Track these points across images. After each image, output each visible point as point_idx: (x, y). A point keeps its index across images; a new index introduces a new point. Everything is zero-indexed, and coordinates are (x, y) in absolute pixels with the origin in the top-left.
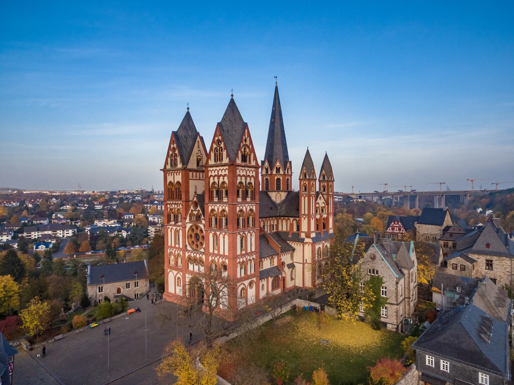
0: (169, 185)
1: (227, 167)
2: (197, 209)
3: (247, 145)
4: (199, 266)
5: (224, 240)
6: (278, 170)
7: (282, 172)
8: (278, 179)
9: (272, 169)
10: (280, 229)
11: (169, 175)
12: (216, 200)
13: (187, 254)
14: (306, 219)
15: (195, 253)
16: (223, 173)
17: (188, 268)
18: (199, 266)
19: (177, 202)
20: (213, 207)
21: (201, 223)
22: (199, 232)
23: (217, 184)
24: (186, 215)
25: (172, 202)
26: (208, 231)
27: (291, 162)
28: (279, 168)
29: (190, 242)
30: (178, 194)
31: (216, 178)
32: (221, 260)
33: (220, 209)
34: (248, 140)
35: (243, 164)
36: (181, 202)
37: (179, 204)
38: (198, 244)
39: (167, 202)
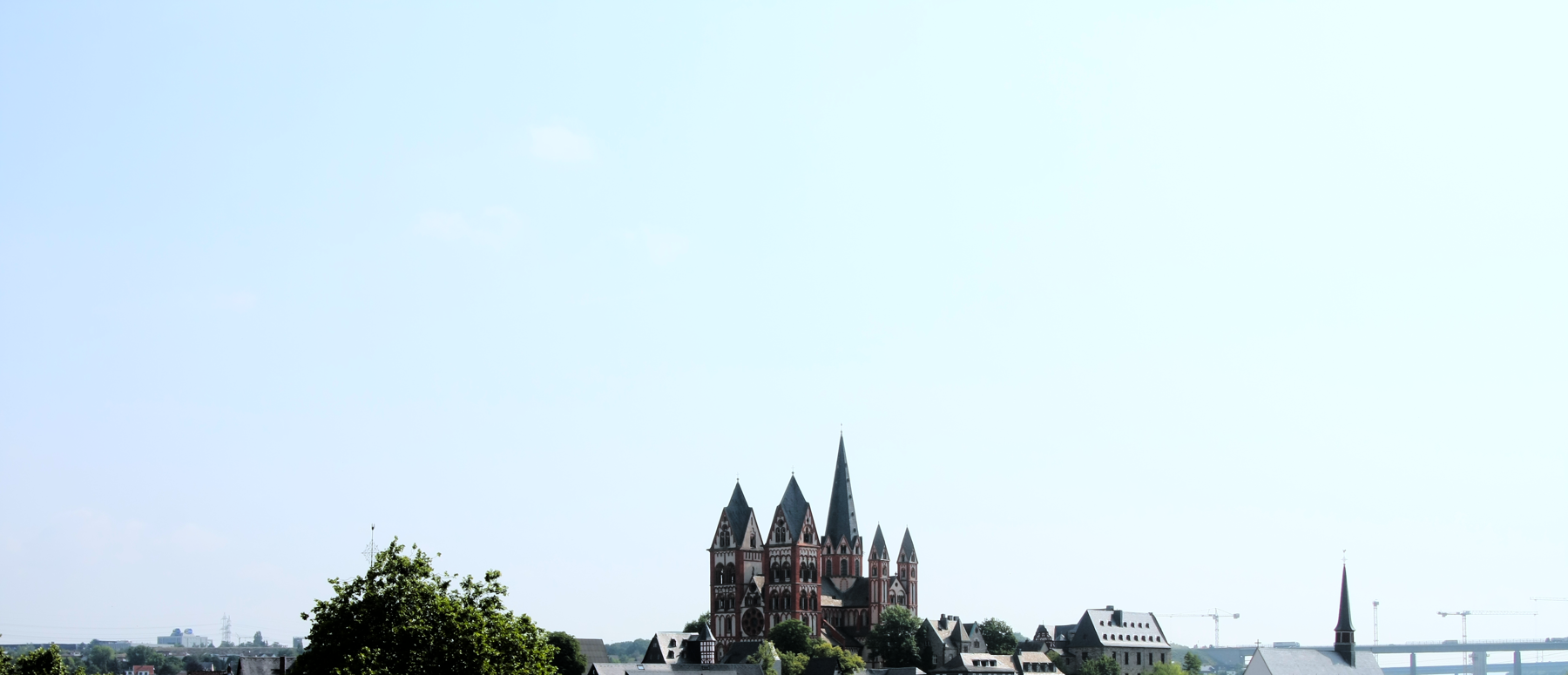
3: (808, 525)
6: (843, 549)
7: (848, 552)
8: (844, 561)
9: (835, 548)
10: (846, 624)
12: (777, 580)
14: (877, 608)
16: (786, 553)
21: (760, 606)
22: (756, 616)
24: (741, 599)
27: (861, 538)
28: (845, 547)
31: (778, 560)
33: (783, 589)
34: (810, 519)
35: (806, 545)
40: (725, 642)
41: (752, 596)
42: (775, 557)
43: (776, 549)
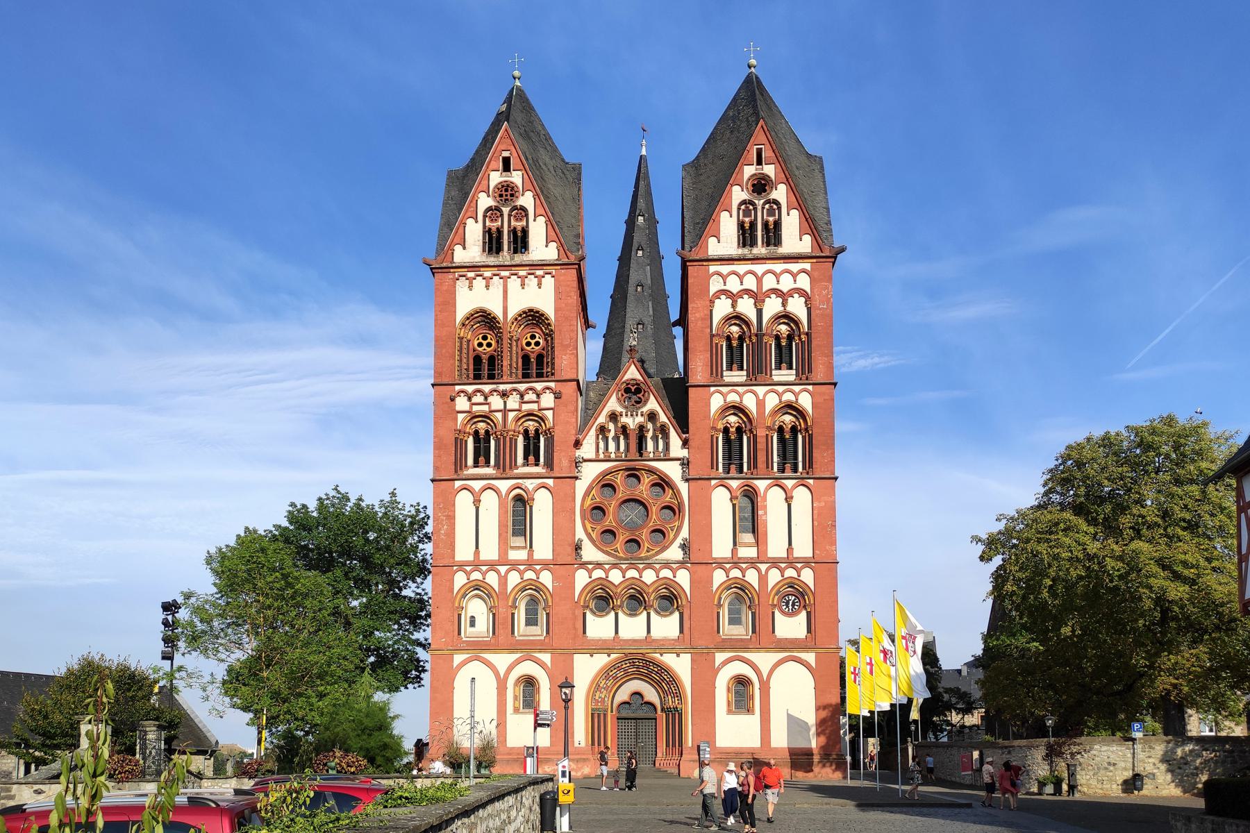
0: (464, 325)
1: (807, 266)
2: (645, 409)
5: (789, 506)
11: (470, 287)
13: (582, 579)
15: (633, 566)
16: (786, 284)
17: (584, 632)
19: (522, 387)
20: (733, 398)
23: (747, 323)
25: (487, 388)
26: (710, 479)
29: (594, 536)
30: (514, 359)
32: (774, 577)
33: (772, 402)
36: (552, 385)
37: (538, 396)
38: (644, 535)
39: (458, 388)
40: (503, 580)
41: (632, 422)
42: (734, 297)
43: (741, 268)
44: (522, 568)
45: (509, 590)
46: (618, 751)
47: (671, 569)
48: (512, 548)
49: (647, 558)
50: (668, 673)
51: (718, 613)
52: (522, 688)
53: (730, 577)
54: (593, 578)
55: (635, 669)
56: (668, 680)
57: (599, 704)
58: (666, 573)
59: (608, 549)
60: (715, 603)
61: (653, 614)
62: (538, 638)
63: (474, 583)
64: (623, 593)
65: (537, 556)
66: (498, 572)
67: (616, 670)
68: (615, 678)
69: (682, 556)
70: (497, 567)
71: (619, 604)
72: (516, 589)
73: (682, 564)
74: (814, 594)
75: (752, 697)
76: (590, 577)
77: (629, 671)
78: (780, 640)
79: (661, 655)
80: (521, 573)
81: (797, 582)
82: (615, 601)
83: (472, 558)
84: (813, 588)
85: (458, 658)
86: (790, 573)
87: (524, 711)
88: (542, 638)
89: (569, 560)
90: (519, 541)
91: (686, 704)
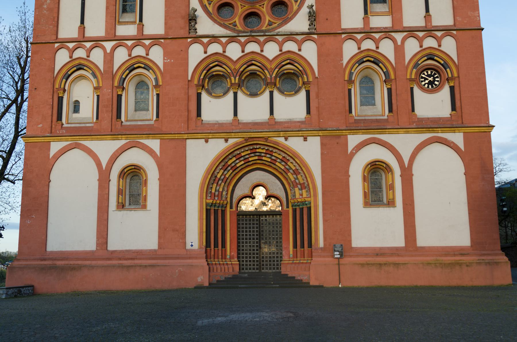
4: (271, 93)
15: (252, 39)
17: (199, 114)
18: (271, 93)
29: (210, 9)
40: (109, 58)
44: (129, 43)
45: (115, 68)
46: (238, 254)
47: (296, 41)
48: (120, 23)
49: (269, 31)
50: (294, 160)
51: (350, 90)
52: (128, 180)
53: (362, 49)
54: (209, 53)
55: (256, 158)
56: (294, 168)
57: (216, 198)
58: (290, 46)
59: (226, 23)
60: (346, 78)
61: (276, 94)
62: (147, 123)
63: (77, 62)
64: (241, 70)
65: (148, 31)
66: (104, 49)
67: (234, 159)
68: (234, 168)
69: (308, 27)
70: (104, 43)
71: (237, 82)
72: (124, 68)
73: (308, 36)
74: (457, 67)
75: (392, 187)
76: (205, 52)
77: (250, 159)
78: (421, 120)
79: (286, 139)
80: (130, 49)
81: (437, 53)
82: (233, 78)
83: (74, 34)
84: (456, 60)
85: (55, 147)
86: (430, 42)
87: (130, 207)
88: (152, 122)
89: (183, 33)
90: (128, 17)
91: (315, 195)
